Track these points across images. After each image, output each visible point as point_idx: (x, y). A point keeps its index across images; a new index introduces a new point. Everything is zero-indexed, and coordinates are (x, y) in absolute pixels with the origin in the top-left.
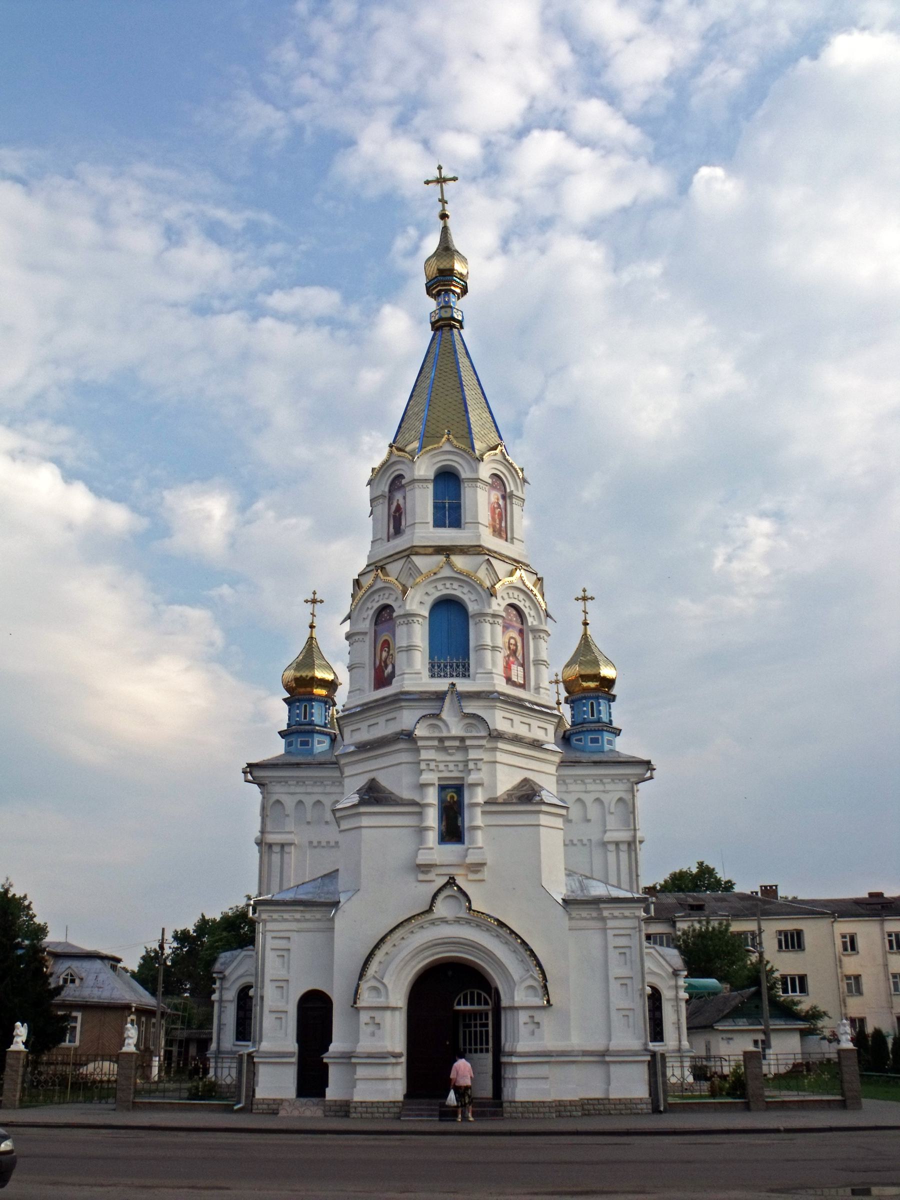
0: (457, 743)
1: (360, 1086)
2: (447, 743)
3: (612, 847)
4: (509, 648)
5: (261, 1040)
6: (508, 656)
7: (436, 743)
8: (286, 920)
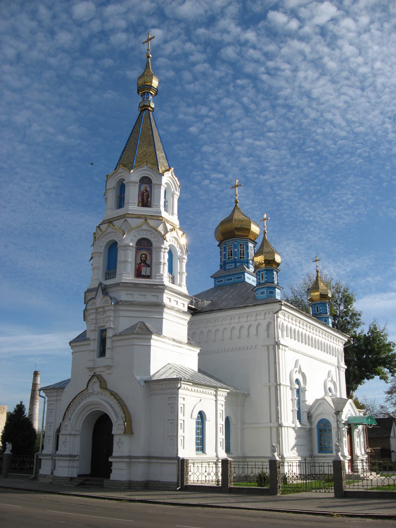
0: (102, 310)
2: (99, 310)
4: (141, 259)
6: (140, 264)
7: (94, 311)
8: (53, 396)
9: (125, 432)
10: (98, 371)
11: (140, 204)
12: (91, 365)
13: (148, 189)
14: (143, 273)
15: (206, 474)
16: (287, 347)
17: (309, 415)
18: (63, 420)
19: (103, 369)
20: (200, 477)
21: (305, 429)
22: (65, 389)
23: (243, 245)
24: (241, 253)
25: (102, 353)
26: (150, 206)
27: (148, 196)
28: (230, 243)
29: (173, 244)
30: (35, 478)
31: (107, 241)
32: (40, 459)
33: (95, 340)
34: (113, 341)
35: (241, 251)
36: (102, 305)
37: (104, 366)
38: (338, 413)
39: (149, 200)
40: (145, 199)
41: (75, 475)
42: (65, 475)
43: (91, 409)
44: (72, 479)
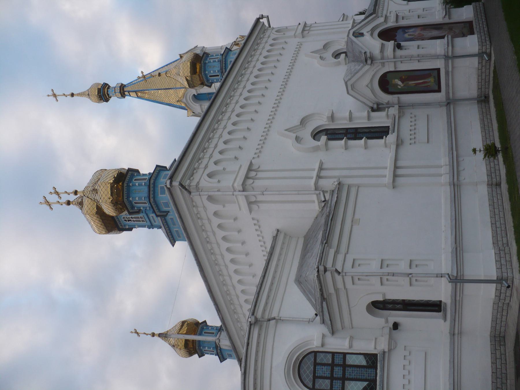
16: (251, 163)
17: (375, 106)
38: (369, 59)
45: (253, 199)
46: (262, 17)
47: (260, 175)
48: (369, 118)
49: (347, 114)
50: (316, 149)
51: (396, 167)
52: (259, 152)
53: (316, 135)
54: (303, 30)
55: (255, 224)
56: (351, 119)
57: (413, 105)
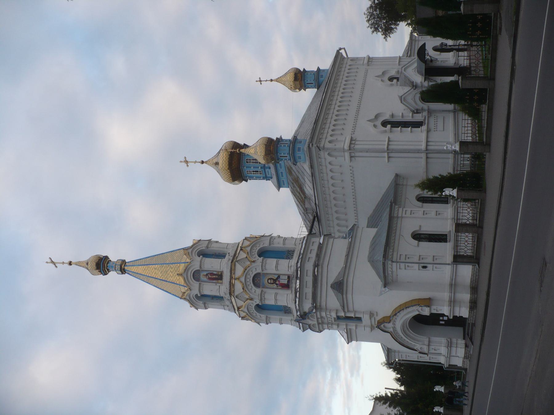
0: (320, 320)
1: (459, 355)
2: (320, 322)
3: (353, 159)
4: (273, 284)
5: (440, 363)
6: (277, 284)
7: (320, 326)
9: (429, 306)
10: (375, 324)
11: (220, 281)
12: (368, 329)
13: (205, 273)
14: (286, 282)
15: (466, 244)
16: (352, 138)
17: (415, 111)
18: (416, 350)
19: (373, 319)
20: (469, 248)
21: (428, 117)
22: (389, 347)
23: (247, 160)
24: (255, 162)
25: (359, 319)
26: (222, 273)
27: (212, 274)
28: (245, 170)
29: (257, 251)
30: (466, 370)
31: (255, 312)
32: (449, 365)
33: (347, 325)
34: (348, 311)
35: (253, 162)
36: (316, 320)
37: (370, 319)
38: (414, 86)
39: (215, 273)
40: (214, 277)
41: (463, 342)
42: (463, 350)
43: (407, 328)
44: (466, 346)
45: (353, 155)
46: (340, 49)
47: (357, 143)
48: (412, 117)
49: (401, 114)
50: (385, 132)
51: (427, 142)
52: (353, 132)
53: (384, 124)
54: (368, 61)
55: (351, 170)
56: (402, 116)
57: (435, 111)
